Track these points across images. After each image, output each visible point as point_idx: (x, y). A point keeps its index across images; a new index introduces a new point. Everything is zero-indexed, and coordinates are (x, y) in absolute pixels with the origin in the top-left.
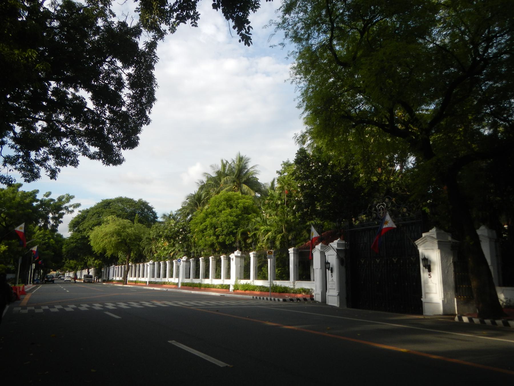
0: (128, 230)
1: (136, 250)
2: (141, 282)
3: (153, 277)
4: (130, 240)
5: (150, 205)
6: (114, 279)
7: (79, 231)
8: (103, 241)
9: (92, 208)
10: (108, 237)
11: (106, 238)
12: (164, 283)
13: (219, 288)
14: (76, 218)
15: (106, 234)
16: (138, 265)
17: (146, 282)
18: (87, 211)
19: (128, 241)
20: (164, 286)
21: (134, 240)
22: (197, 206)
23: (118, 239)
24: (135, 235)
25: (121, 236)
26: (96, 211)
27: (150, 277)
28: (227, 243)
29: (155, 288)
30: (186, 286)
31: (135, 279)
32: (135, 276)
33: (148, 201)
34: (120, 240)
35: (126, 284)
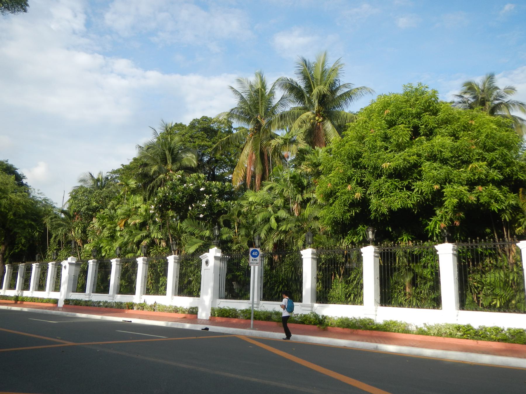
0: (13, 196)
1: (25, 238)
2: (33, 299)
3: (83, 289)
4: (14, 215)
5: (19, 172)
12: (131, 306)
13: (451, 335)
16: (22, 266)
17: (56, 301)
19: (10, 216)
20: (130, 311)
21: (25, 217)
22: (166, 163)
24: (25, 207)
27: (68, 291)
28: (495, 207)
29: (135, 321)
30: (302, 323)
31: (12, 293)
32: (12, 286)
33: (16, 166)
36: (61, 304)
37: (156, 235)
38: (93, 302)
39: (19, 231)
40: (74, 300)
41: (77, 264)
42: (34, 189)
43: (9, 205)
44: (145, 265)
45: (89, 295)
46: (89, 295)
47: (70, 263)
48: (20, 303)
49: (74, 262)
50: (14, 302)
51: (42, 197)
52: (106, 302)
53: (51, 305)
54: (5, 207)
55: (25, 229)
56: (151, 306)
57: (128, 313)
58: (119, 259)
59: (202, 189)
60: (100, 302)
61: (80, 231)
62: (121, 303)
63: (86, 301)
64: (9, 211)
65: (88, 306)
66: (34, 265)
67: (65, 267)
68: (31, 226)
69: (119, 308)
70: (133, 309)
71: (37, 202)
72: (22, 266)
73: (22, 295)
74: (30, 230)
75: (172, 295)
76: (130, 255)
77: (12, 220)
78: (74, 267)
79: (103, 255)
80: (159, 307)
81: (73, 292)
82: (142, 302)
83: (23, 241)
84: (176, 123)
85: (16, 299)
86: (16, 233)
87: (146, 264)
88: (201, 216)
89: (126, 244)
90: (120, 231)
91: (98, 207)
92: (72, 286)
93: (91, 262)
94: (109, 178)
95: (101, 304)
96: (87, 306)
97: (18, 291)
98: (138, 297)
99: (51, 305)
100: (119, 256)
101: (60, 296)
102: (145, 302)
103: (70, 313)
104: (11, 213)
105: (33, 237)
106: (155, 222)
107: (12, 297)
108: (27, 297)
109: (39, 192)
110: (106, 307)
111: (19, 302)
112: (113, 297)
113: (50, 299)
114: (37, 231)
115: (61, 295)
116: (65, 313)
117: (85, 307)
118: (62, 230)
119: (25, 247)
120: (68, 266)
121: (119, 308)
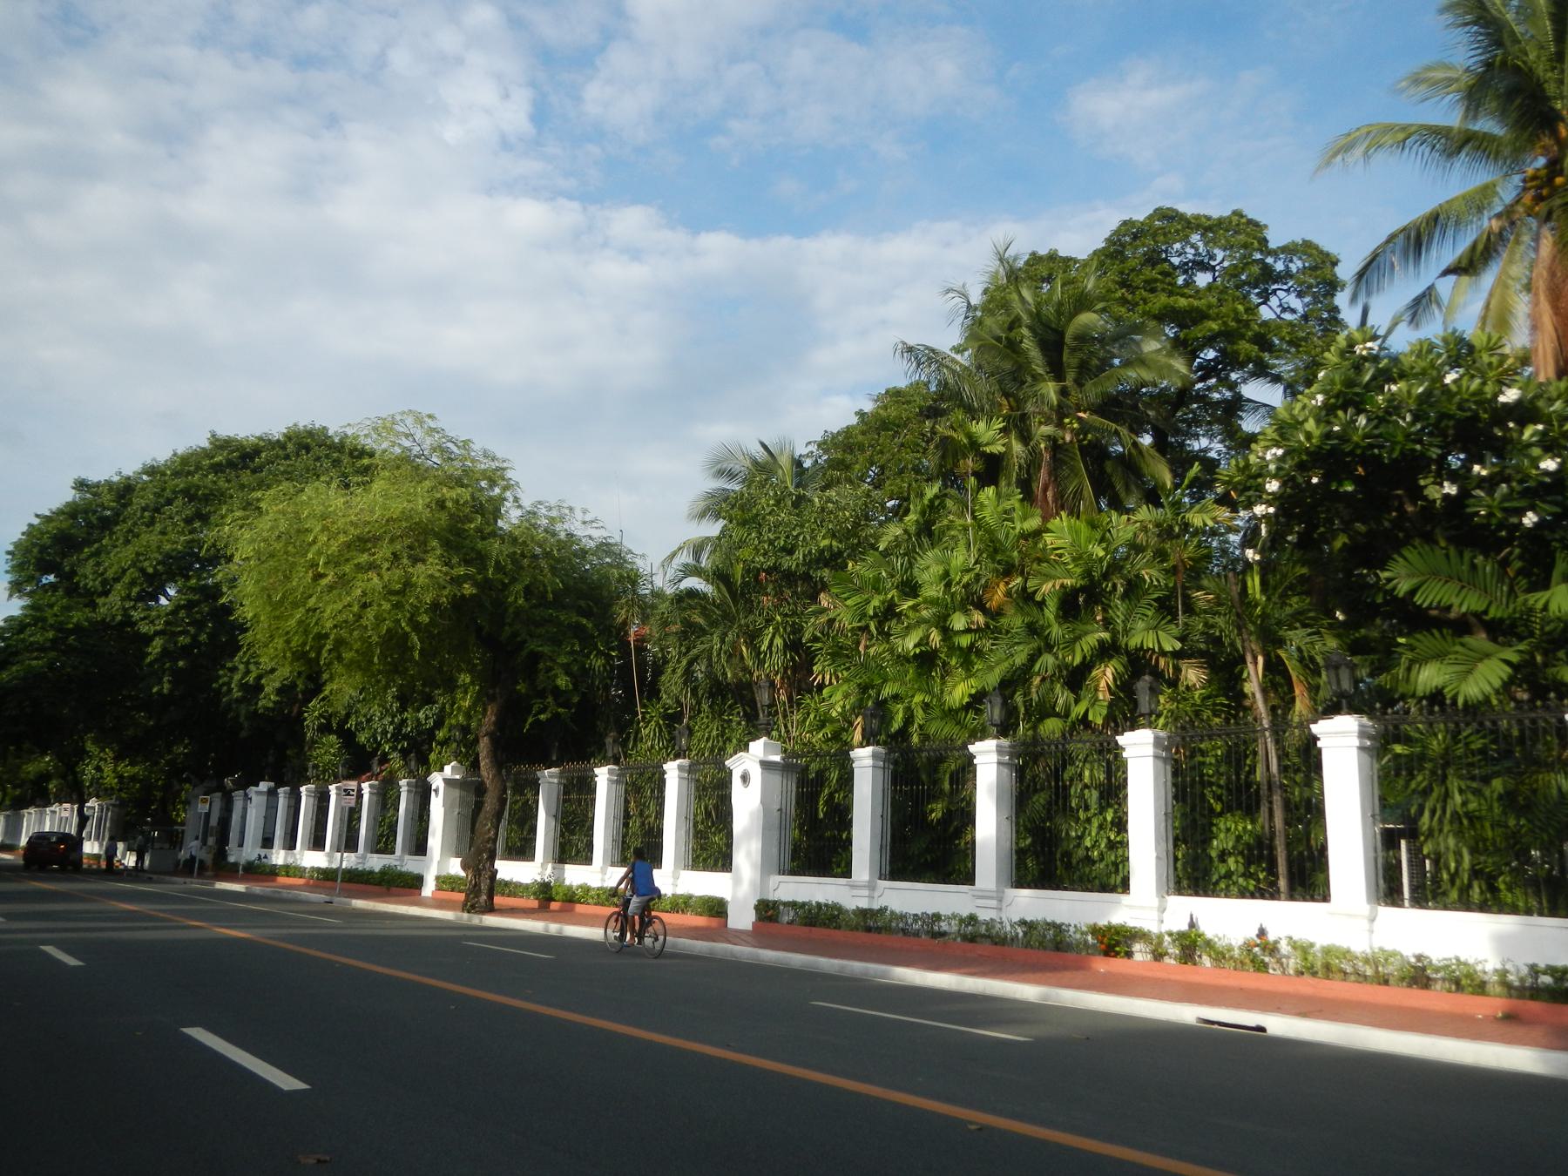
4: (528, 591)
6: (279, 857)
7: (70, 586)
8: (343, 582)
9: (152, 471)
10: (383, 552)
11: (372, 566)
12: (1115, 941)
14: (47, 519)
15: (363, 542)
16: (549, 778)
17: (717, 908)
18: (124, 491)
19: (516, 598)
20: (1116, 965)
21: (558, 602)
23: (457, 581)
25: (479, 559)
26: (181, 483)
27: (765, 869)
29: (1279, 1025)
34: (468, 589)
35: (490, 909)
36: (742, 918)
37: (1144, 635)
38: (903, 917)
39: (546, 649)
40: (804, 904)
41: (785, 768)
42: (571, 509)
43: (512, 556)
44: (1161, 764)
45: (871, 887)
46: (862, 886)
47: (766, 765)
48: (561, 911)
49: (777, 758)
50: (534, 903)
51: (596, 534)
52: (972, 919)
53: (701, 921)
54: (499, 567)
55: (559, 643)
56: (1248, 947)
57: (1108, 975)
58: (1005, 742)
59: (1510, 395)
60: (937, 917)
61: (778, 641)
62: (1058, 928)
63: (864, 913)
64: (514, 580)
65: (873, 929)
66: (603, 776)
67: (745, 778)
68: (578, 631)
69: (1048, 949)
70: (1129, 955)
71: (584, 553)
72: (549, 778)
73: (560, 880)
74: (577, 648)
75: (1369, 901)
76: (1051, 726)
77: (518, 612)
78: (776, 779)
79: (896, 725)
80: (1176, 944)
81: (782, 872)
82: (1184, 927)
83: (562, 681)
84: (1034, 254)
85: (546, 896)
86: (535, 657)
87: (1165, 760)
88: (1530, 519)
89: (1012, 683)
90: (968, 631)
91: (840, 553)
92: (775, 851)
93: (864, 758)
94: (807, 463)
95: (944, 926)
96: (869, 930)
97: (543, 865)
98: (1146, 903)
99: (701, 921)
100: (1004, 730)
101: (741, 884)
102: (1192, 925)
103: (836, 962)
104: (519, 587)
105: (586, 672)
106: (1134, 588)
107: (527, 887)
108: (586, 889)
109: (588, 518)
110: (972, 939)
111: (554, 906)
112: (991, 896)
113: (690, 897)
114: (600, 653)
115: (737, 882)
116: (744, 951)
117: (862, 936)
118: (723, 641)
119: (566, 705)
120: (756, 773)
121: (1048, 949)
